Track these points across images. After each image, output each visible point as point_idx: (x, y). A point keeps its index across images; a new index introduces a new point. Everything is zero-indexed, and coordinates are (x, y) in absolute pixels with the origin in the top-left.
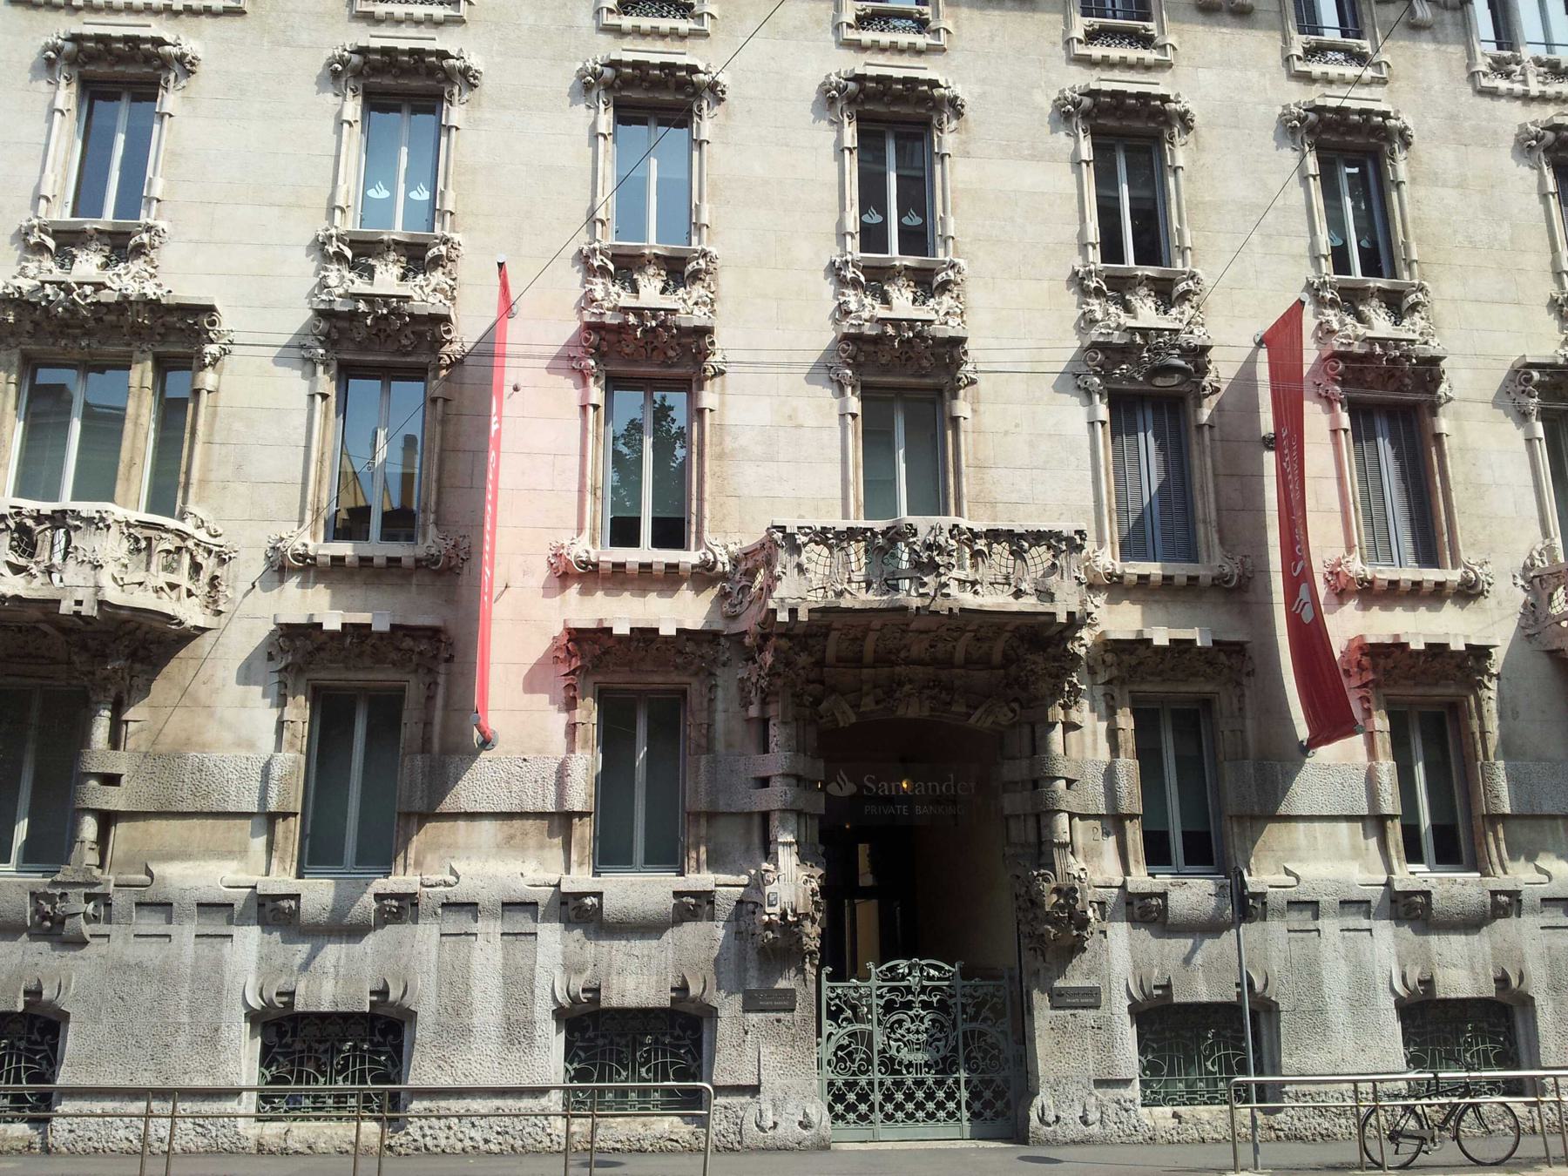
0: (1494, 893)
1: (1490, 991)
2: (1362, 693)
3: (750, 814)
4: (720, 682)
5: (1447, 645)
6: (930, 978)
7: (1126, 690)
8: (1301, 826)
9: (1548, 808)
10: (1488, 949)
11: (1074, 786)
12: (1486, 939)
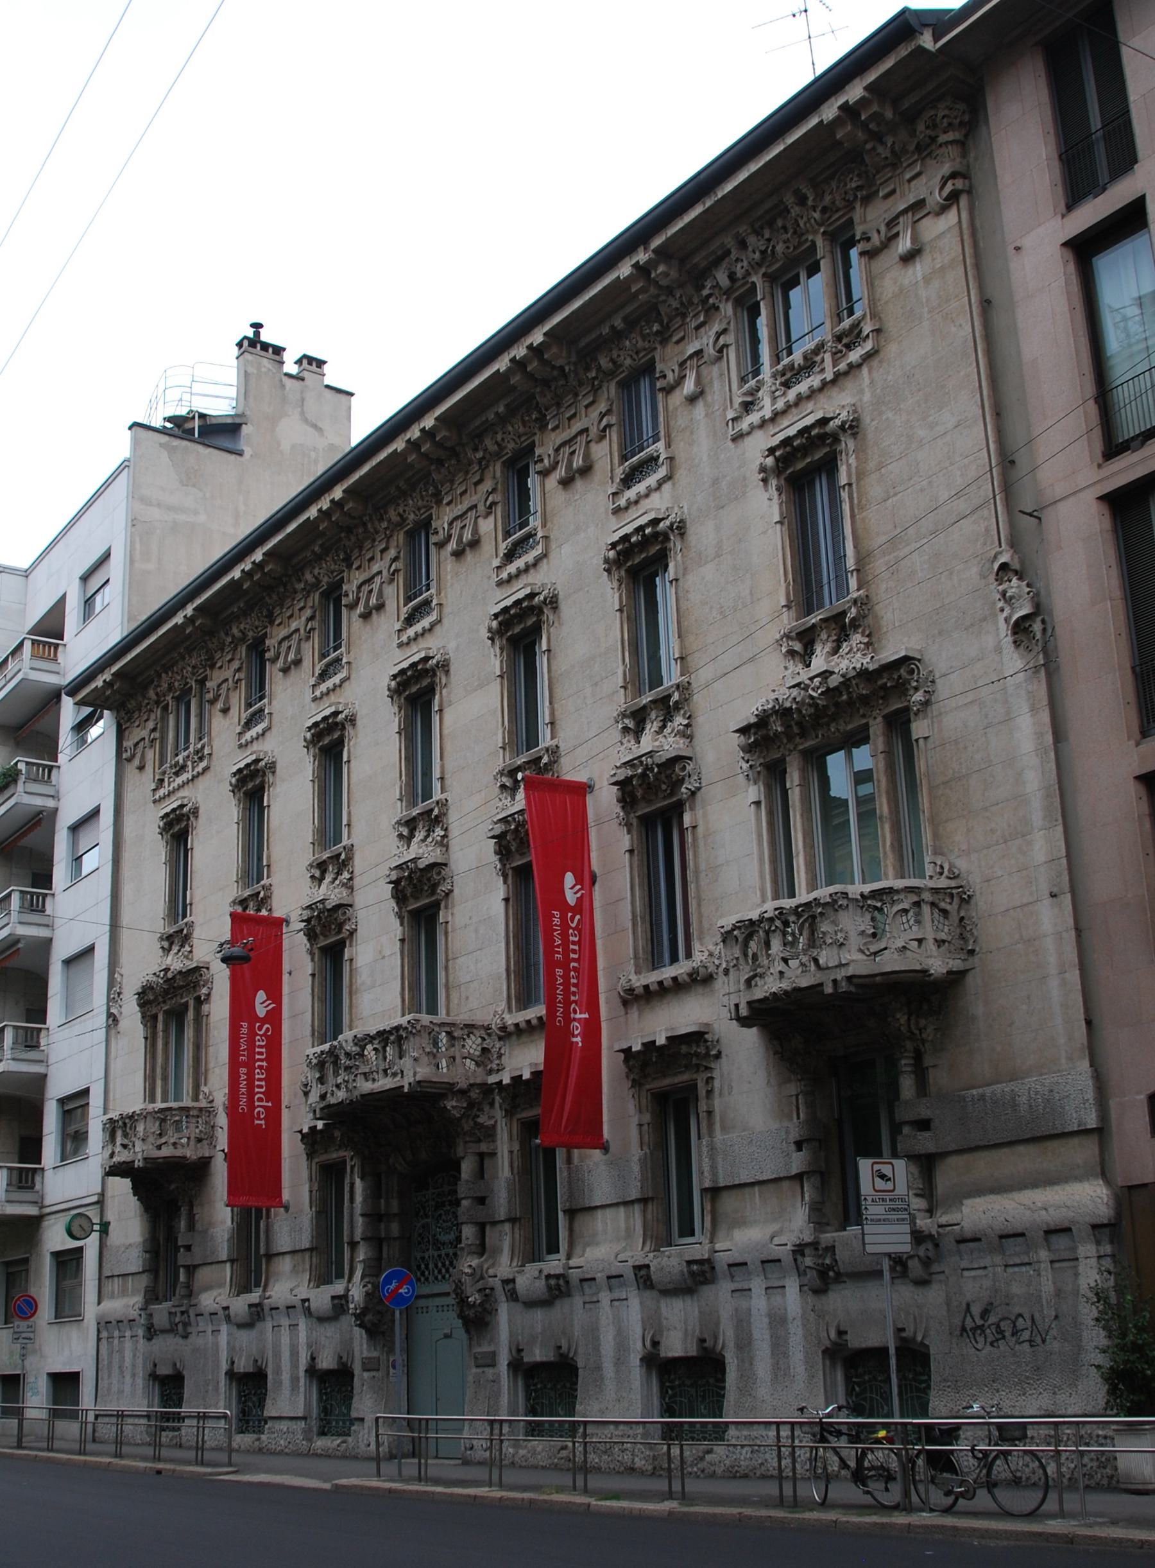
0: (689, 1263)
1: (693, 1352)
8: (599, 1214)
9: (745, 1178)
10: (696, 1312)
12: (696, 1304)
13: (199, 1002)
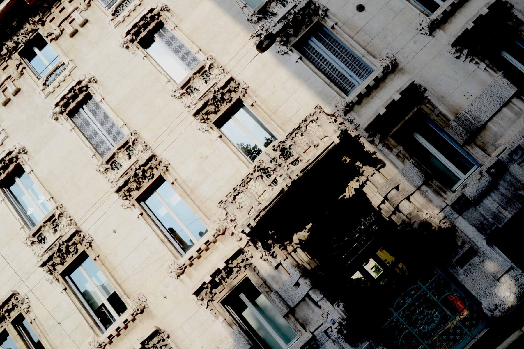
2: (469, 59)
3: (303, 300)
4: (255, 264)
5: (481, 15)
6: (414, 294)
7: (389, 138)
8: (489, 124)
11: (400, 188)
13: (18, 322)
